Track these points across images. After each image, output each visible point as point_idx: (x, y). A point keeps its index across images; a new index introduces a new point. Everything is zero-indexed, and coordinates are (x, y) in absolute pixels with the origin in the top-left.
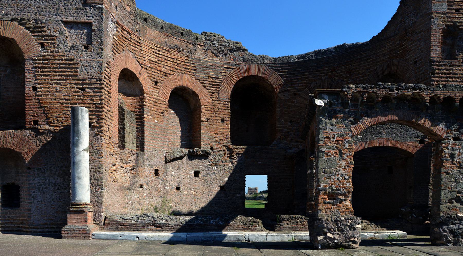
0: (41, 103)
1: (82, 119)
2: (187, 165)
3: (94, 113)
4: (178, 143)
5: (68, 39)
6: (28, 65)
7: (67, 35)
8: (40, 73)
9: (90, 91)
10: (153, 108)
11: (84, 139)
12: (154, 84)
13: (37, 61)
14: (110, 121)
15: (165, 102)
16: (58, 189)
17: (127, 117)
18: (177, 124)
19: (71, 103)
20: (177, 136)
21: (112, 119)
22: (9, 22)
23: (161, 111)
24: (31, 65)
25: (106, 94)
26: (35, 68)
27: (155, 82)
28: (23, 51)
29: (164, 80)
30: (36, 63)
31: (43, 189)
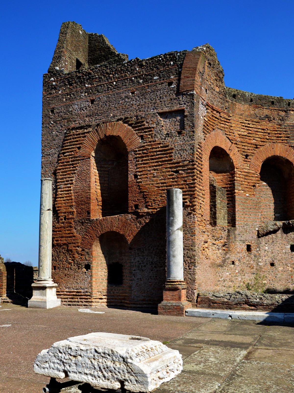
0: (141, 189)
1: (176, 200)
2: (282, 239)
3: (187, 193)
4: (272, 216)
5: (163, 128)
6: (130, 157)
7: (162, 124)
8: (140, 162)
9: (183, 172)
10: (244, 181)
11: (178, 219)
12: (245, 157)
13: (138, 152)
14: (202, 199)
15: (257, 174)
16: (155, 267)
17: (218, 194)
18: (270, 196)
19: (166, 186)
20: (270, 208)
21: (204, 197)
23: (253, 184)
25: (198, 174)
26: (136, 158)
27: (245, 156)
28: (127, 145)
29: (255, 152)
30: (137, 154)
31: (142, 267)
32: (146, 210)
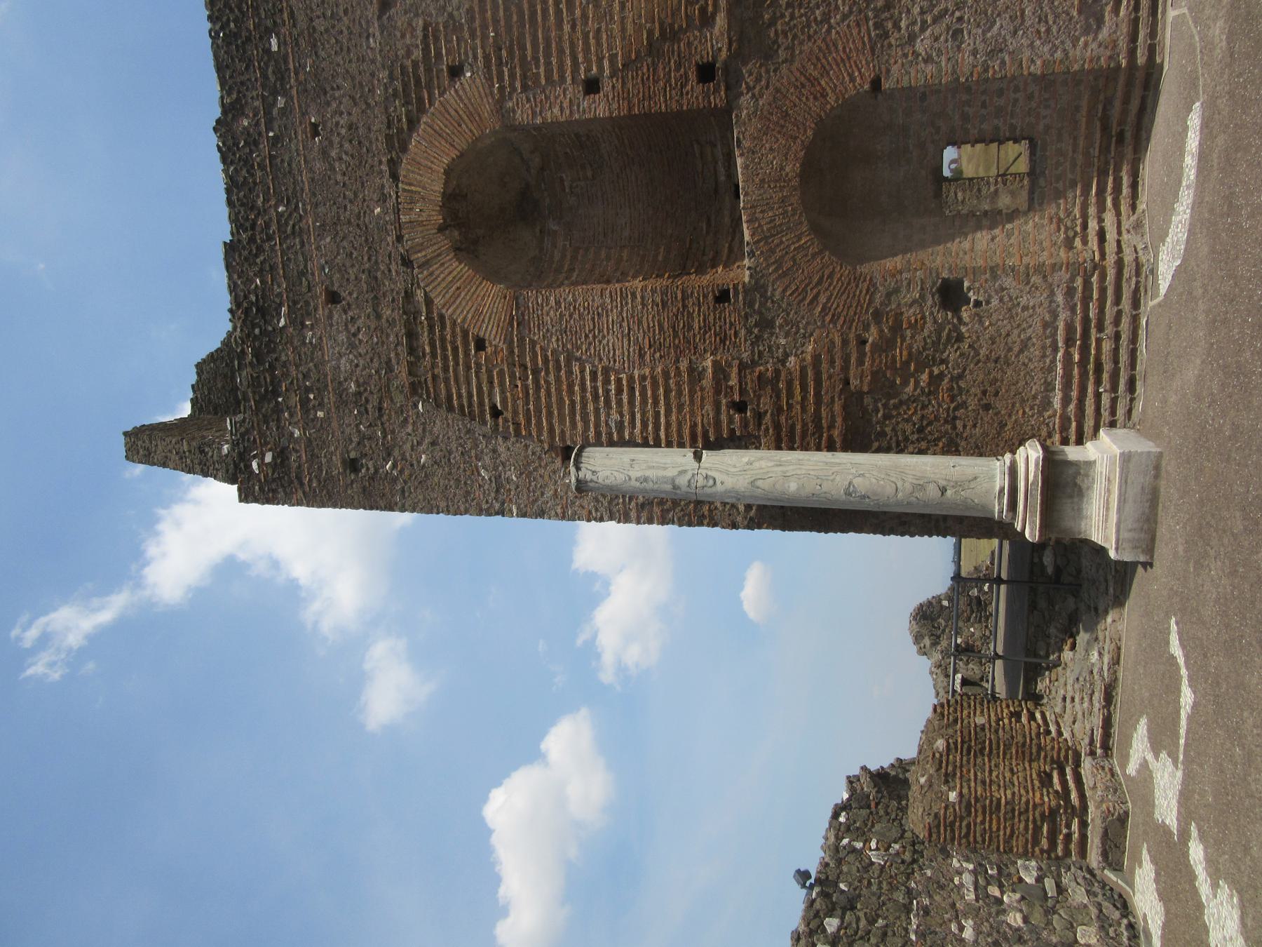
0: (638, 53)
6: (522, 115)
8: (542, 70)
22: (400, 185)
24: (518, 104)
26: (525, 88)
30: (514, 89)
32: (721, 21)
